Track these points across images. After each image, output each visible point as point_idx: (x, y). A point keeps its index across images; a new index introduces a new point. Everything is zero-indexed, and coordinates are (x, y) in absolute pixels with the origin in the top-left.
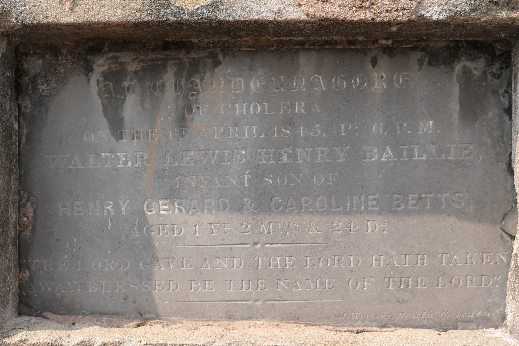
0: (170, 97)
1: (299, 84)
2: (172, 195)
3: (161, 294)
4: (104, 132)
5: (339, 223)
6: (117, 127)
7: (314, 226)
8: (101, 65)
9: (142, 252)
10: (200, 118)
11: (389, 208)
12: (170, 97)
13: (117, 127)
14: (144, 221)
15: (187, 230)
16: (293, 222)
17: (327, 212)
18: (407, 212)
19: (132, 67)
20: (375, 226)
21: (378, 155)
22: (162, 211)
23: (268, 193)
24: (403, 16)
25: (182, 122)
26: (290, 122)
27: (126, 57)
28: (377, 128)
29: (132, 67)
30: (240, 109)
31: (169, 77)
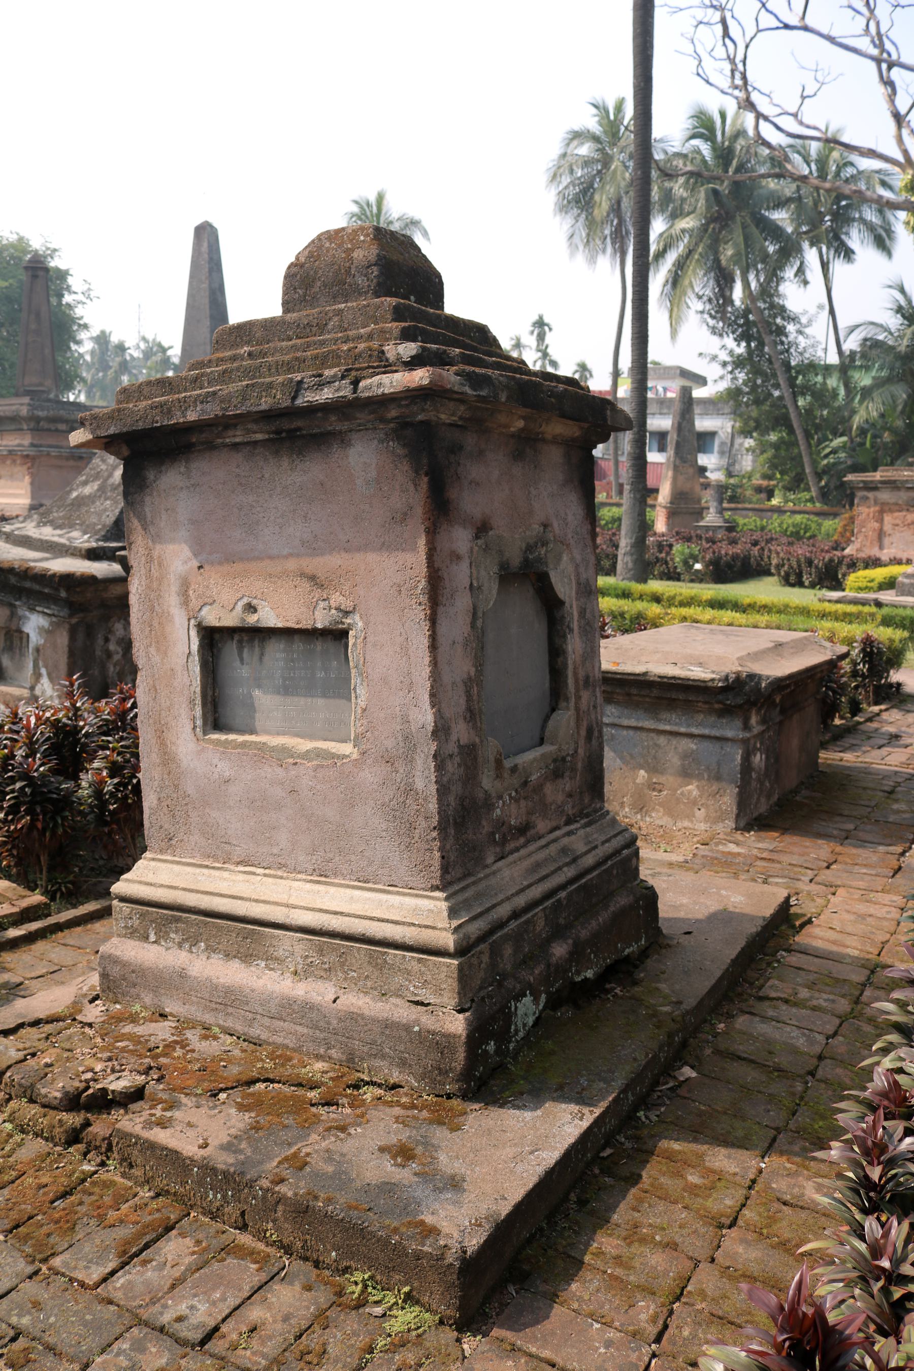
0: (257, 649)
1: (295, 647)
2: (259, 687)
3: (258, 725)
4: (238, 663)
5: (309, 700)
6: (242, 660)
7: (302, 701)
8: (236, 637)
9: (251, 707)
10: (266, 658)
11: (324, 696)
12: (257, 649)
13: (242, 660)
14: (251, 697)
15: (265, 701)
16: (296, 699)
17: (305, 696)
18: (329, 697)
19: (245, 638)
20: (321, 701)
21: (320, 674)
22: (257, 693)
23: (287, 689)
24: (309, 627)
25: (261, 659)
26: (292, 661)
27: (243, 635)
28: (319, 664)
29: (245, 638)
30: (278, 655)
31: (256, 642)
